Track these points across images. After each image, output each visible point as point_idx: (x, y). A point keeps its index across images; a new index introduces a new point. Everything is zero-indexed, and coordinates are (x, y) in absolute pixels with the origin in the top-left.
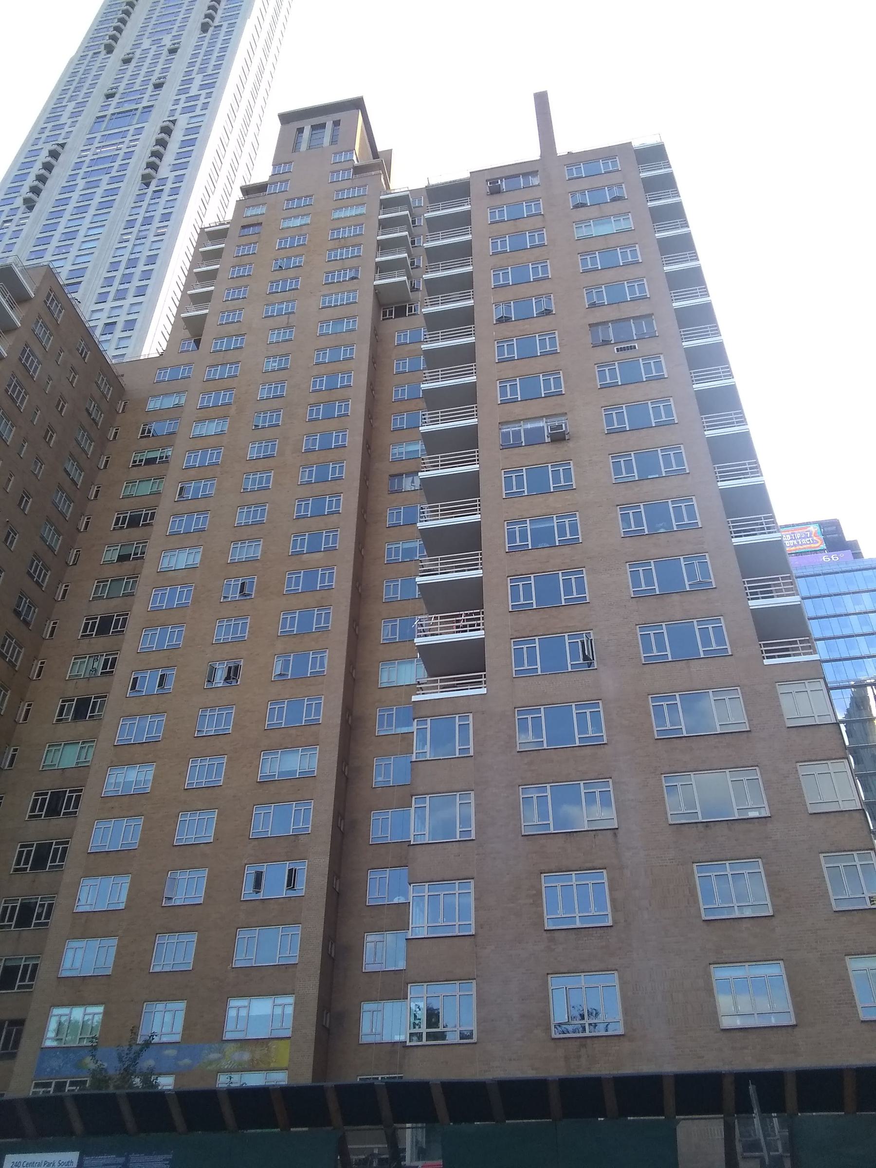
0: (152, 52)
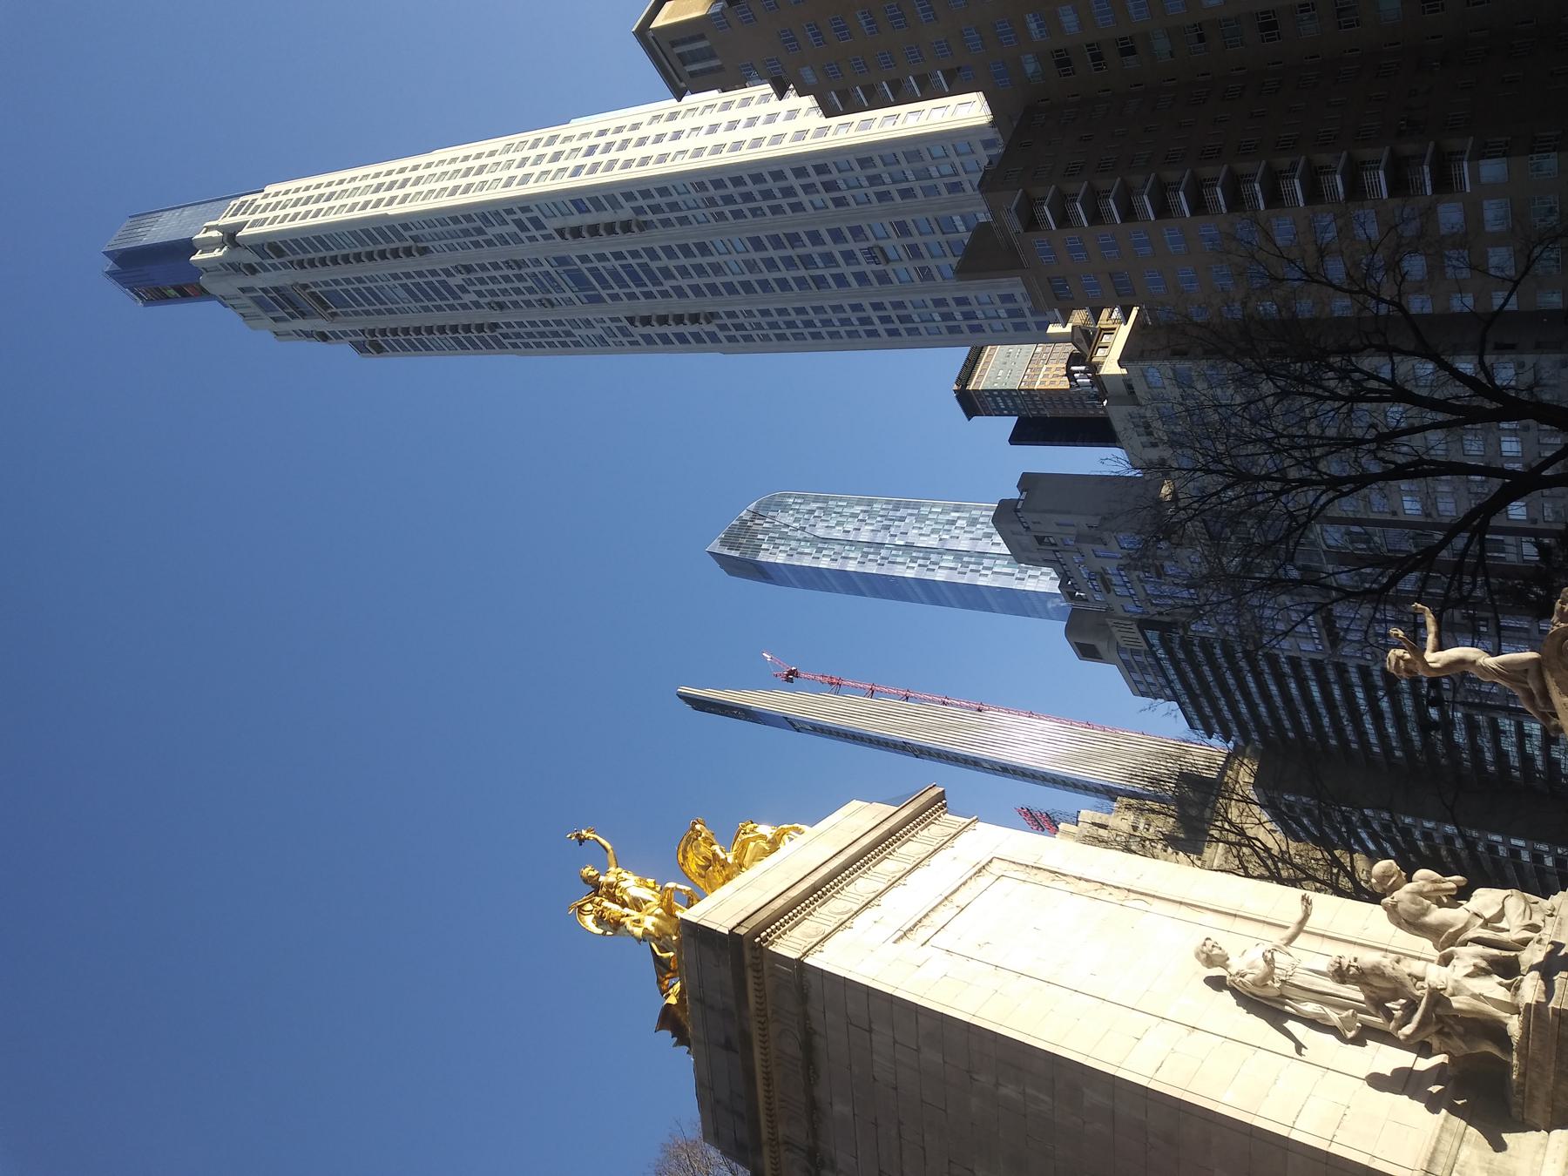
0: (479, 287)
